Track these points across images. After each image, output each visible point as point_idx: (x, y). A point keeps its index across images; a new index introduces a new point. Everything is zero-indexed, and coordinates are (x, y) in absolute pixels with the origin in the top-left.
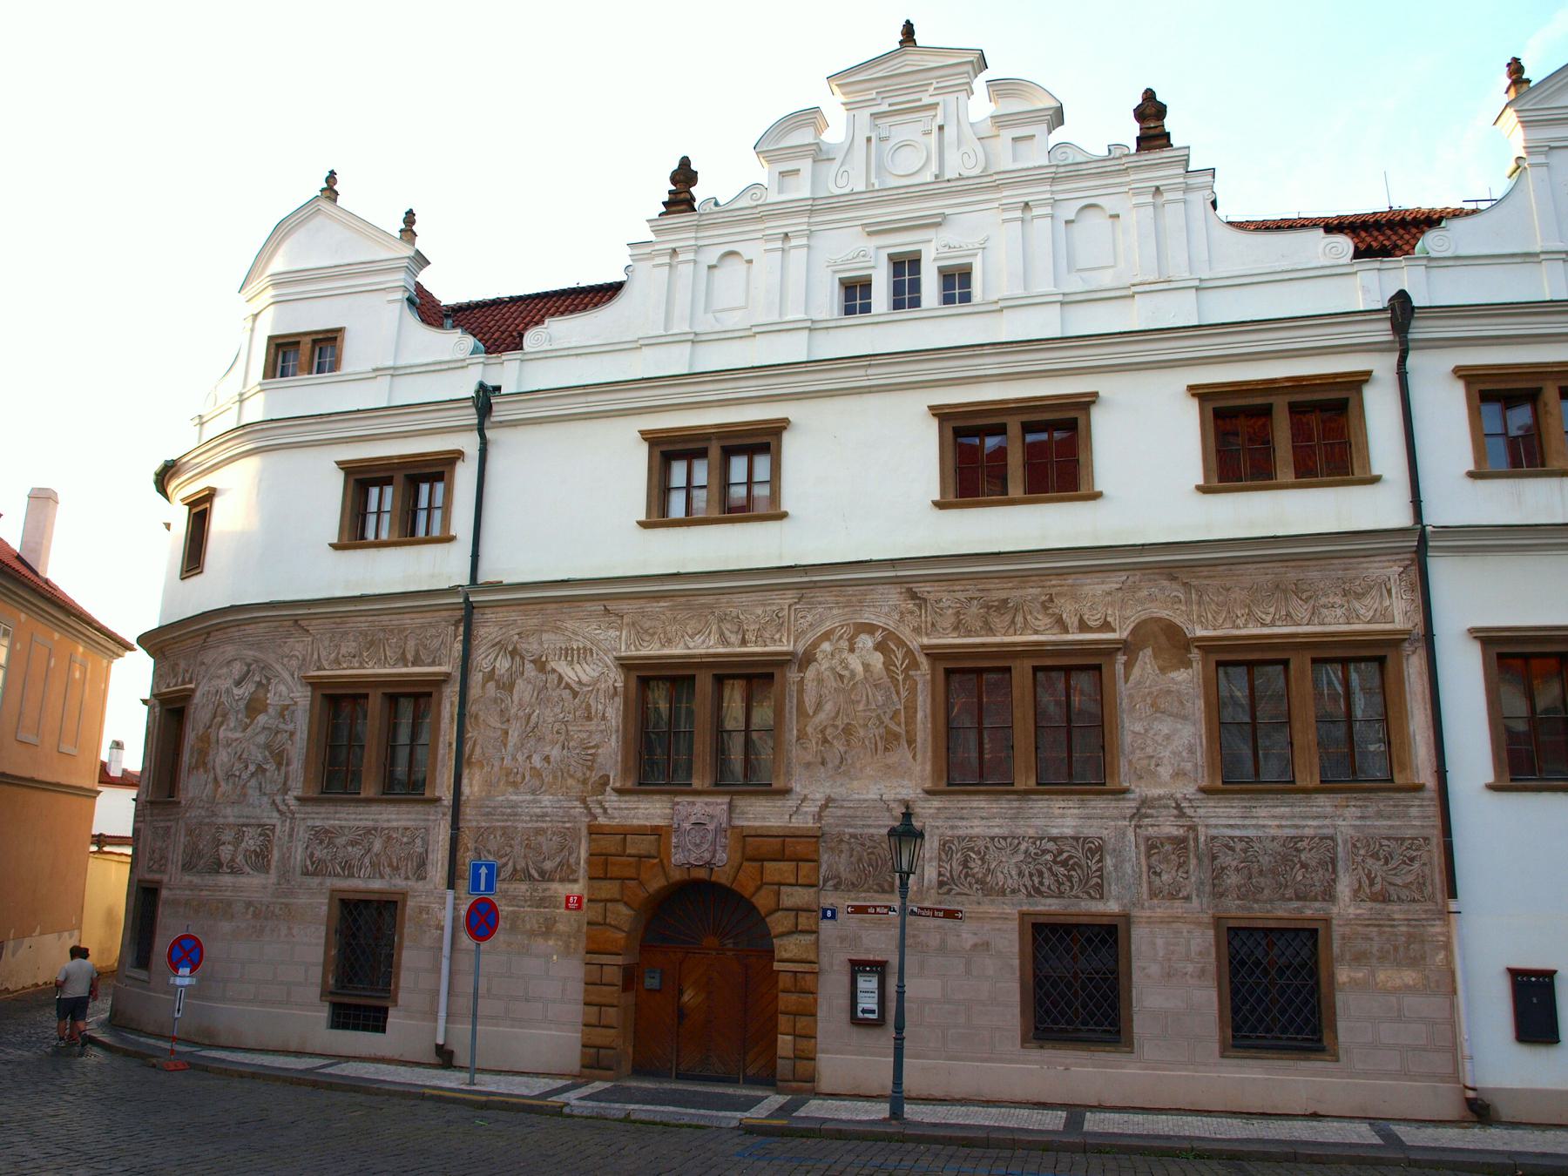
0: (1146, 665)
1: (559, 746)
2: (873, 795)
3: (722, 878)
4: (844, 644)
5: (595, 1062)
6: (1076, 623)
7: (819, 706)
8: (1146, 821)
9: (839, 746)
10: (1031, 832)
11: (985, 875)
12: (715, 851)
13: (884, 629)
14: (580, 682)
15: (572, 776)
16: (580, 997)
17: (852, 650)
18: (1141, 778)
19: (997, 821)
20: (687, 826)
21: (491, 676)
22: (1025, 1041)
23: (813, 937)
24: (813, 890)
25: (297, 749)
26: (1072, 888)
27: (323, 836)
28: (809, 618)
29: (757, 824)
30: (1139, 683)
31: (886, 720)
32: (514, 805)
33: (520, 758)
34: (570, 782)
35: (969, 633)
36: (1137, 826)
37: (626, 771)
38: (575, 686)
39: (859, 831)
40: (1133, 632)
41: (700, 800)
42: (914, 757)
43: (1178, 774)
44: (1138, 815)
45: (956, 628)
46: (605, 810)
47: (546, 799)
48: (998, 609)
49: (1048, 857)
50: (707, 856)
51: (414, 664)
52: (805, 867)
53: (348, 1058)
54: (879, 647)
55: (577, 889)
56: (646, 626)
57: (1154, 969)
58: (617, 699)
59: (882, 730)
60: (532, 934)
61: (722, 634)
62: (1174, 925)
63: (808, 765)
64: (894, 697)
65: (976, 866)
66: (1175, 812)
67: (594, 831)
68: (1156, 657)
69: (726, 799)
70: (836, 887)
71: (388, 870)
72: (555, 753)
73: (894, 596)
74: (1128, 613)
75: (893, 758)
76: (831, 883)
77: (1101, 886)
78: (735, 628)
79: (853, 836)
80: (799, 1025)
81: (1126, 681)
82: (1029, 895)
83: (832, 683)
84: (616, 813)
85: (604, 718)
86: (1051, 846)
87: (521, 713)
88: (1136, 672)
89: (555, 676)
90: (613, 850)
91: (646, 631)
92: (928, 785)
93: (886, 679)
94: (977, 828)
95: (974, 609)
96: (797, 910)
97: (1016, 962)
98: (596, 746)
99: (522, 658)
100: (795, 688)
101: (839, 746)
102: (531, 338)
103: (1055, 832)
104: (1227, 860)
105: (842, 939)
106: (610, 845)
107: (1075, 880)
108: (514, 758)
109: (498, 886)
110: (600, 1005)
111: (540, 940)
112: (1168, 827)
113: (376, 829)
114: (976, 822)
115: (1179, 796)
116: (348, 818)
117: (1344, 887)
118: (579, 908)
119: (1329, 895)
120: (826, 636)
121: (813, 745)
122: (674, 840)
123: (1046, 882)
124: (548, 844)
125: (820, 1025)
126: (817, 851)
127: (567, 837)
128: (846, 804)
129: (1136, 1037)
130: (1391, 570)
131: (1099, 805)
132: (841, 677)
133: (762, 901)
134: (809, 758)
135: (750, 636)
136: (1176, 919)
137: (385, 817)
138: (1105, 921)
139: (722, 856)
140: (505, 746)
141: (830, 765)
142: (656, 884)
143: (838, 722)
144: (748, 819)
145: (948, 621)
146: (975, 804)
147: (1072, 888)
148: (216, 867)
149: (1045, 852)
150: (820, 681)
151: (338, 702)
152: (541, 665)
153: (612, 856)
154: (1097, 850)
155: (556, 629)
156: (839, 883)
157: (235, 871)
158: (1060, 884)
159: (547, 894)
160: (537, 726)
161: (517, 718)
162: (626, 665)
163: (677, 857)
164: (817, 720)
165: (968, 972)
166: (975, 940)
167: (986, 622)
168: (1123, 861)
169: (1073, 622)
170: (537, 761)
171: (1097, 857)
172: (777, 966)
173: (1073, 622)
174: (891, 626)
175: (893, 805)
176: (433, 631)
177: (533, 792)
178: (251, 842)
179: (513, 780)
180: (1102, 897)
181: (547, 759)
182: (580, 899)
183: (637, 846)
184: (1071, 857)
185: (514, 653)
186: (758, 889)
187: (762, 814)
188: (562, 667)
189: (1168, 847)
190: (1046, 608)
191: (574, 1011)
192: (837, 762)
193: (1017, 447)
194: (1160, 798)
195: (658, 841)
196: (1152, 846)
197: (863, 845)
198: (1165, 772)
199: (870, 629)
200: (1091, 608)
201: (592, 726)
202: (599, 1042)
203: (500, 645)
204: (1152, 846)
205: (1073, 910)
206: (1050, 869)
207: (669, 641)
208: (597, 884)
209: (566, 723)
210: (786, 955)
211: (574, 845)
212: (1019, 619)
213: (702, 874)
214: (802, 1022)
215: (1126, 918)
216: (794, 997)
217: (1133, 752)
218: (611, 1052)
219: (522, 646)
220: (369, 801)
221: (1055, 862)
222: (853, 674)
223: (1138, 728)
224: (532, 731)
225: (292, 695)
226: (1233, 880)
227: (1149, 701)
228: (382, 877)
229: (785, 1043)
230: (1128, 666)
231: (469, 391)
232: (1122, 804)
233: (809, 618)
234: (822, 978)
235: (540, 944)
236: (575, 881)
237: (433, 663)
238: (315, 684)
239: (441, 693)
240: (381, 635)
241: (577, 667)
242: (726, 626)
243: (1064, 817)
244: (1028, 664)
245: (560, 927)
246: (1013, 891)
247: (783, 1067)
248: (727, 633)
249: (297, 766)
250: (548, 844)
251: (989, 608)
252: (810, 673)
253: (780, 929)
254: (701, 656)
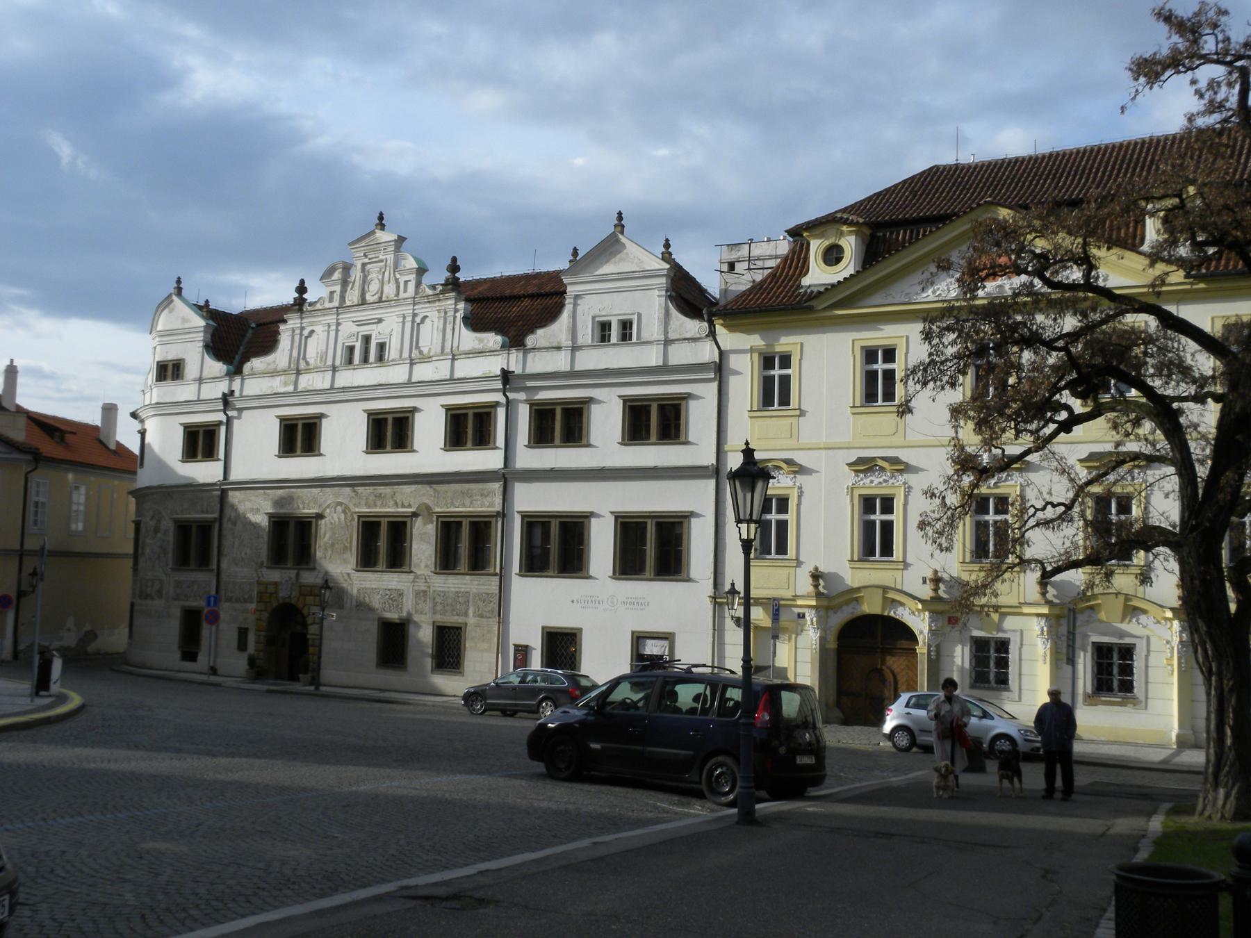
0: (418, 522)
3: (293, 602)
25: (170, 547)
27: (178, 584)
43: (426, 566)
51: (207, 512)
54: (344, 511)
67: (259, 583)
72: (248, 551)
73: (348, 490)
94: (367, 585)
95: (372, 498)
102: (247, 368)
104: (438, 599)
112: (422, 586)
116: (187, 577)
117: (471, 612)
119: (466, 614)
130: (497, 486)
131: (403, 576)
133: (305, 611)
142: (275, 604)
145: (363, 502)
148: (147, 597)
151: (183, 529)
153: (266, 593)
155: (250, 501)
157: (152, 598)
178: (157, 587)
183: (271, 589)
193: (390, 431)
198: (423, 565)
204: (417, 594)
225: (168, 525)
226: (439, 607)
231: (220, 396)
238: (176, 521)
243: (392, 581)
249: (170, 555)
252: (323, 522)
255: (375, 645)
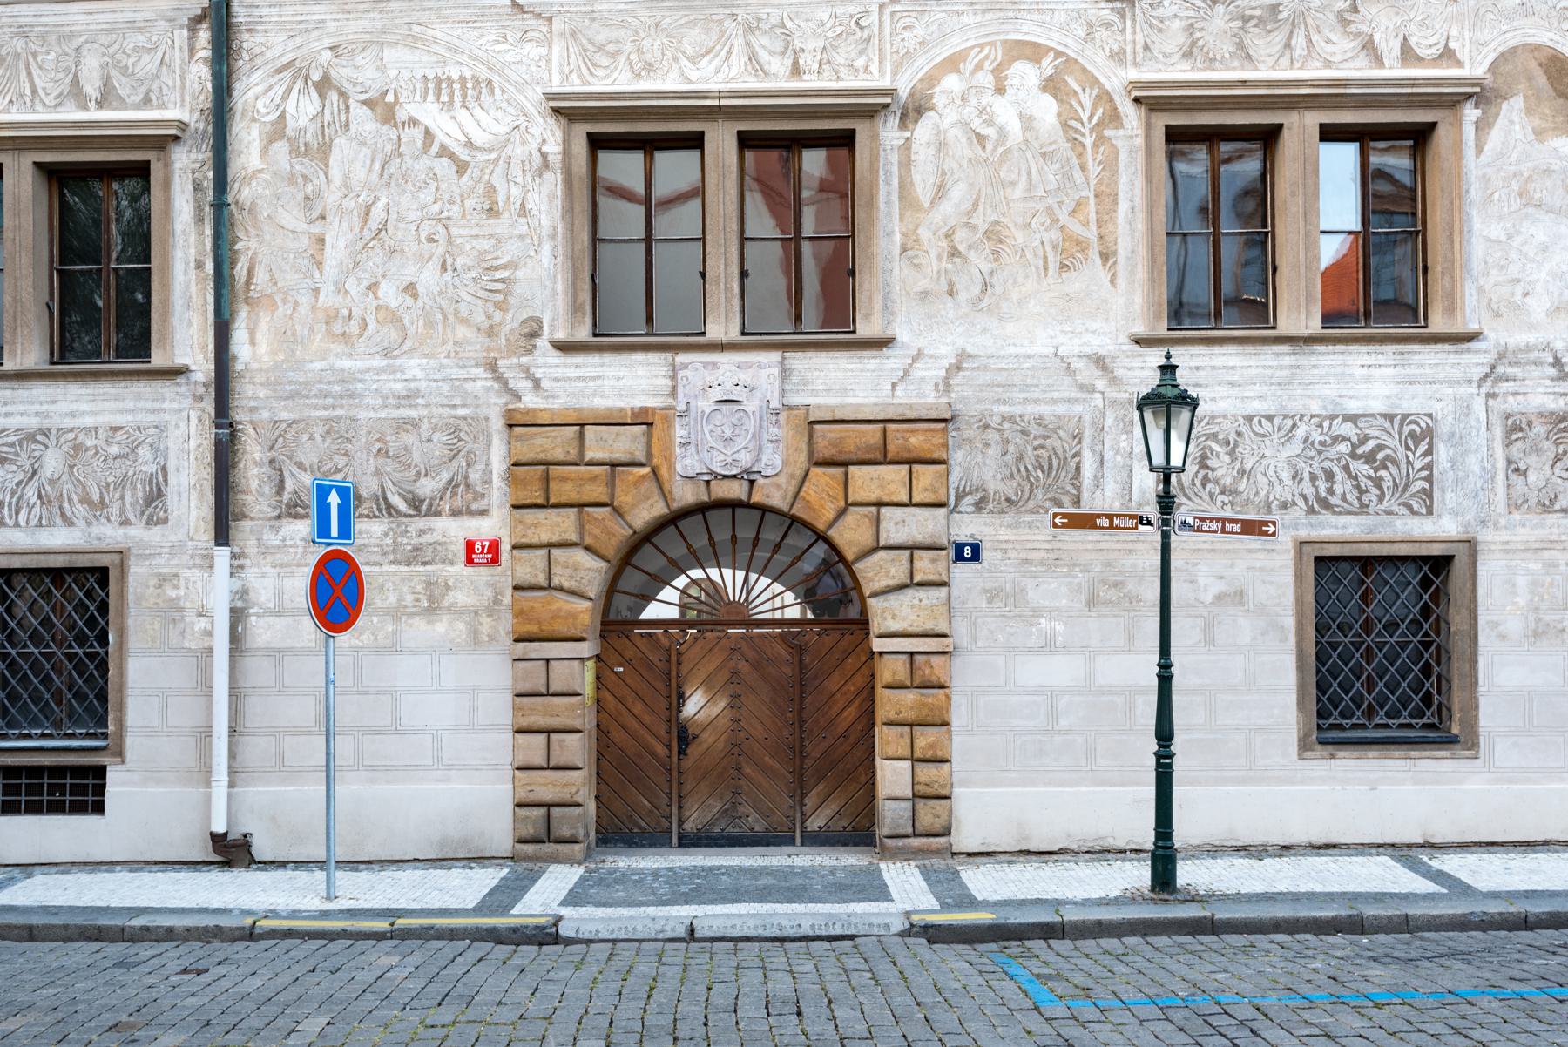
1: (434, 265)
2: (1042, 346)
3: (774, 495)
4: (986, 79)
5: (540, 836)
6: (1397, 51)
7: (941, 191)
8: (1505, 387)
9: (980, 261)
10: (1315, 407)
11: (1236, 480)
12: (760, 449)
13: (1059, 54)
14: (470, 144)
15: (464, 321)
16: (506, 718)
17: (1000, 90)
18: (1498, 315)
19: (1258, 389)
20: (706, 406)
21: (278, 130)
22: (1304, 746)
23: (944, 590)
24: (943, 511)
26: (1381, 498)
28: (920, 31)
29: (832, 401)
30: (1500, 155)
31: (1064, 218)
32: (346, 378)
33: (353, 287)
34: (462, 332)
35: (1211, 62)
36: (1489, 395)
37: (576, 309)
38: (463, 154)
39: (1016, 410)
40: (1493, 68)
41: (726, 359)
42: (1113, 281)
44: (1491, 375)
45: (1188, 54)
46: (537, 384)
47: (414, 366)
48: (1261, 21)
49: (1344, 448)
50: (745, 459)
51: (100, 105)
52: (926, 474)
53: (27, 868)
54: (1052, 86)
55: (492, 526)
56: (600, 38)
57: (1514, 626)
58: (548, 176)
59: (1055, 235)
60: (397, 613)
61: (753, 57)
62: (1546, 554)
63: (925, 295)
64: (1078, 177)
65: (1221, 465)
66: (1553, 372)
68: (1529, 111)
69: (775, 356)
70: (979, 506)
71: (81, 510)
72: (429, 279)
74: (1485, 35)
75: (1076, 282)
76: (969, 500)
77: (1429, 495)
78: (778, 45)
79: (1010, 419)
80: (921, 743)
81: (1479, 149)
82: (1311, 511)
83: (962, 147)
84: (558, 388)
85: (523, 211)
86: (1348, 429)
87: (349, 203)
88: (1495, 137)
89: (417, 133)
90: (559, 454)
91: (601, 48)
92: (1141, 329)
93: (1063, 145)
96: (912, 548)
97: (1290, 621)
98: (512, 265)
99: (343, 95)
100: (894, 158)
101: (980, 261)
103: (1353, 407)
105: (992, 595)
106: (556, 445)
107: (1387, 484)
108: (341, 289)
109: (359, 526)
110: (549, 731)
111: (419, 623)
113: (46, 433)
114: (1222, 391)
115: (1559, 345)
118: (495, 561)
120: (952, 63)
121: (933, 260)
122: (679, 432)
123: (1339, 488)
124: (426, 449)
125: (957, 740)
126: (945, 445)
127: (460, 438)
128: (993, 364)
129: (1482, 732)
132: (981, 139)
133: (850, 534)
134: (924, 284)
135: (808, 61)
136: (1550, 544)
137: (63, 407)
138: (1436, 550)
139: (772, 460)
140: (319, 264)
141: (963, 296)
142: (647, 511)
143: (977, 220)
144: (815, 393)
145: (1174, 40)
146: (1219, 361)
147: (1381, 498)
149: (1337, 439)
150: (941, 146)
152: (384, 109)
154: (1422, 436)
156: (983, 500)
158: (1362, 492)
159: (427, 538)
160: (384, 227)
161: (341, 212)
162: (566, 112)
163: (688, 462)
164: (937, 216)
165: (1209, 641)
166: (1217, 587)
167: (1241, 46)
168: (1467, 452)
169: (1390, 47)
170: (389, 294)
171: (1423, 447)
172: (877, 645)
173: (1390, 47)
174: (1072, 48)
175: (1077, 364)
176: (140, 39)
177: (387, 353)
179: (341, 328)
180: (1430, 512)
181: (411, 289)
182: (494, 547)
184: (1380, 447)
185: (324, 85)
186: (842, 513)
187: (838, 382)
188: (429, 113)
189: (1539, 429)
190: (1344, 23)
191: (500, 746)
192: (976, 290)
194: (1528, 349)
195: (649, 436)
196: (1514, 428)
197: (1025, 433)
198: (1538, 306)
199: (1034, 52)
200: (1423, 25)
201: (501, 226)
202: (547, 795)
203: (293, 70)
204: (1514, 428)
205: (1384, 533)
206: (1346, 468)
207: (649, 67)
208: (530, 516)
209: (445, 222)
210: (895, 626)
211: (478, 448)
212: (1299, 41)
213: (736, 491)
214: (925, 739)
215: (1471, 544)
216: (910, 696)
217: (1486, 274)
218: (577, 811)
219: (342, 73)
220: (22, 376)
221: (1353, 455)
222: (1003, 134)
223: (1496, 231)
224: (375, 236)
227: (1515, 186)
228: (71, 524)
229: (893, 777)
230: (1482, 126)
232: (1466, 359)
233: (920, 31)
234: (957, 662)
235: (419, 630)
236: (483, 513)
237: (146, 102)
239: (168, 165)
240: (19, 45)
241: (462, 114)
242: (760, 41)
243: (1369, 379)
244: (1313, 119)
245: (461, 598)
246: (1284, 506)
247: (892, 815)
248: (763, 56)
250: (426, 449)
251: (1246, 19)
252: (923, 130)
253: (884, 582)
254: (720, 94)
255: (1290, 661)
